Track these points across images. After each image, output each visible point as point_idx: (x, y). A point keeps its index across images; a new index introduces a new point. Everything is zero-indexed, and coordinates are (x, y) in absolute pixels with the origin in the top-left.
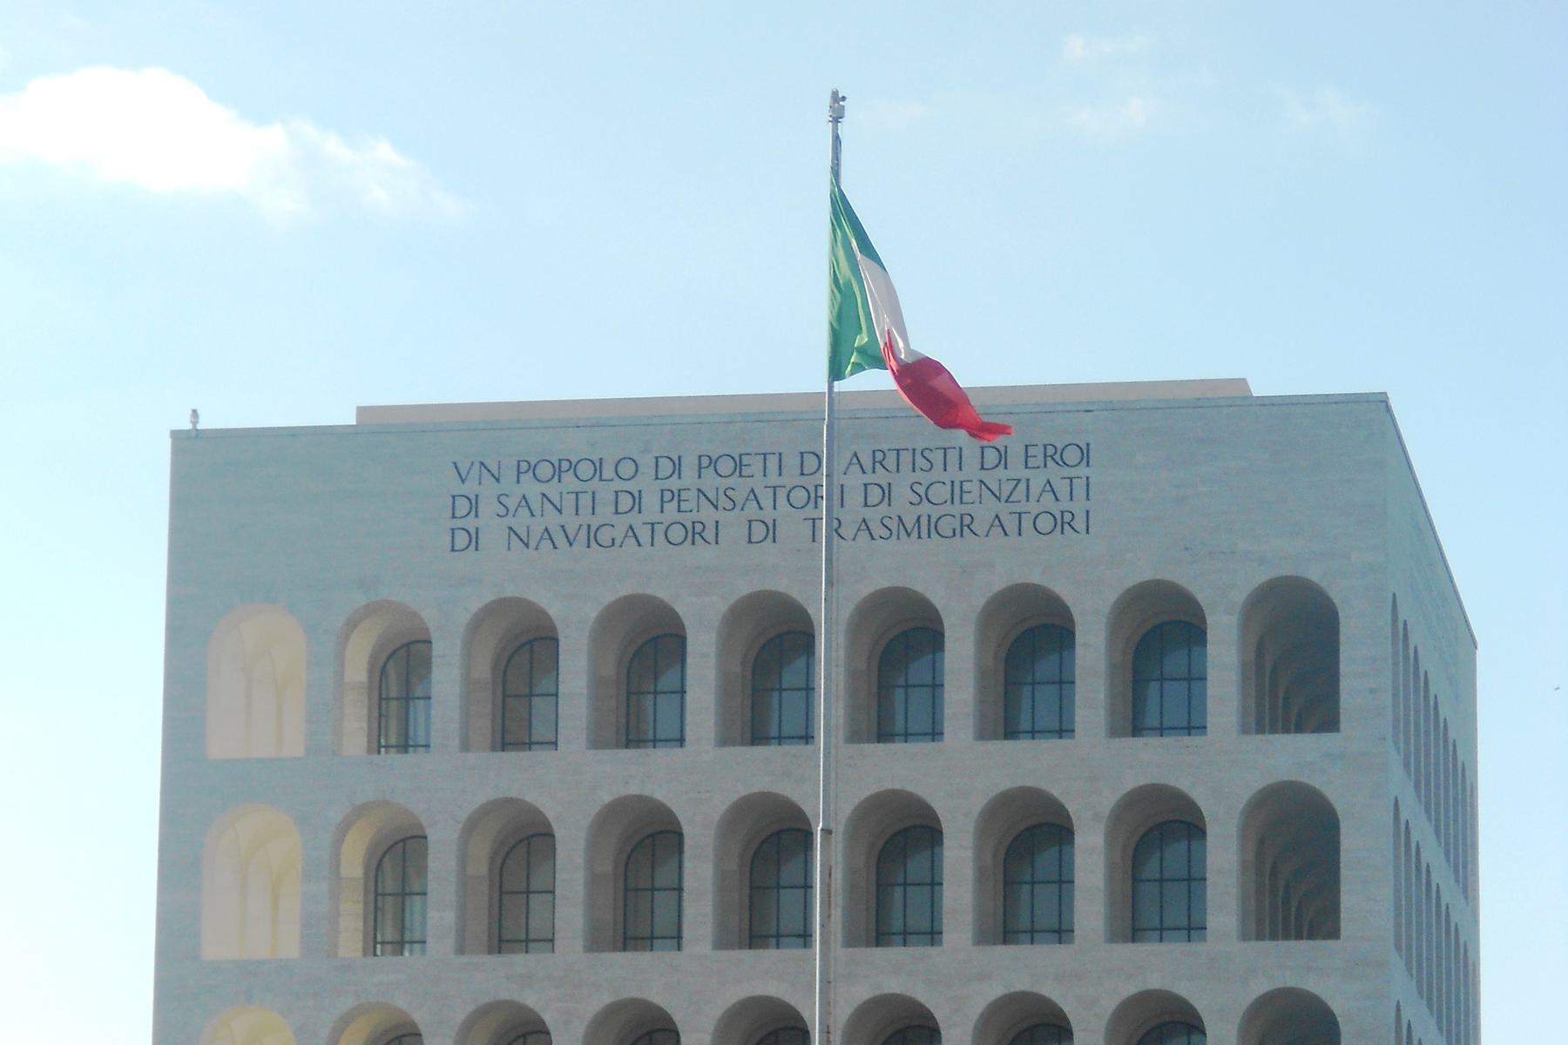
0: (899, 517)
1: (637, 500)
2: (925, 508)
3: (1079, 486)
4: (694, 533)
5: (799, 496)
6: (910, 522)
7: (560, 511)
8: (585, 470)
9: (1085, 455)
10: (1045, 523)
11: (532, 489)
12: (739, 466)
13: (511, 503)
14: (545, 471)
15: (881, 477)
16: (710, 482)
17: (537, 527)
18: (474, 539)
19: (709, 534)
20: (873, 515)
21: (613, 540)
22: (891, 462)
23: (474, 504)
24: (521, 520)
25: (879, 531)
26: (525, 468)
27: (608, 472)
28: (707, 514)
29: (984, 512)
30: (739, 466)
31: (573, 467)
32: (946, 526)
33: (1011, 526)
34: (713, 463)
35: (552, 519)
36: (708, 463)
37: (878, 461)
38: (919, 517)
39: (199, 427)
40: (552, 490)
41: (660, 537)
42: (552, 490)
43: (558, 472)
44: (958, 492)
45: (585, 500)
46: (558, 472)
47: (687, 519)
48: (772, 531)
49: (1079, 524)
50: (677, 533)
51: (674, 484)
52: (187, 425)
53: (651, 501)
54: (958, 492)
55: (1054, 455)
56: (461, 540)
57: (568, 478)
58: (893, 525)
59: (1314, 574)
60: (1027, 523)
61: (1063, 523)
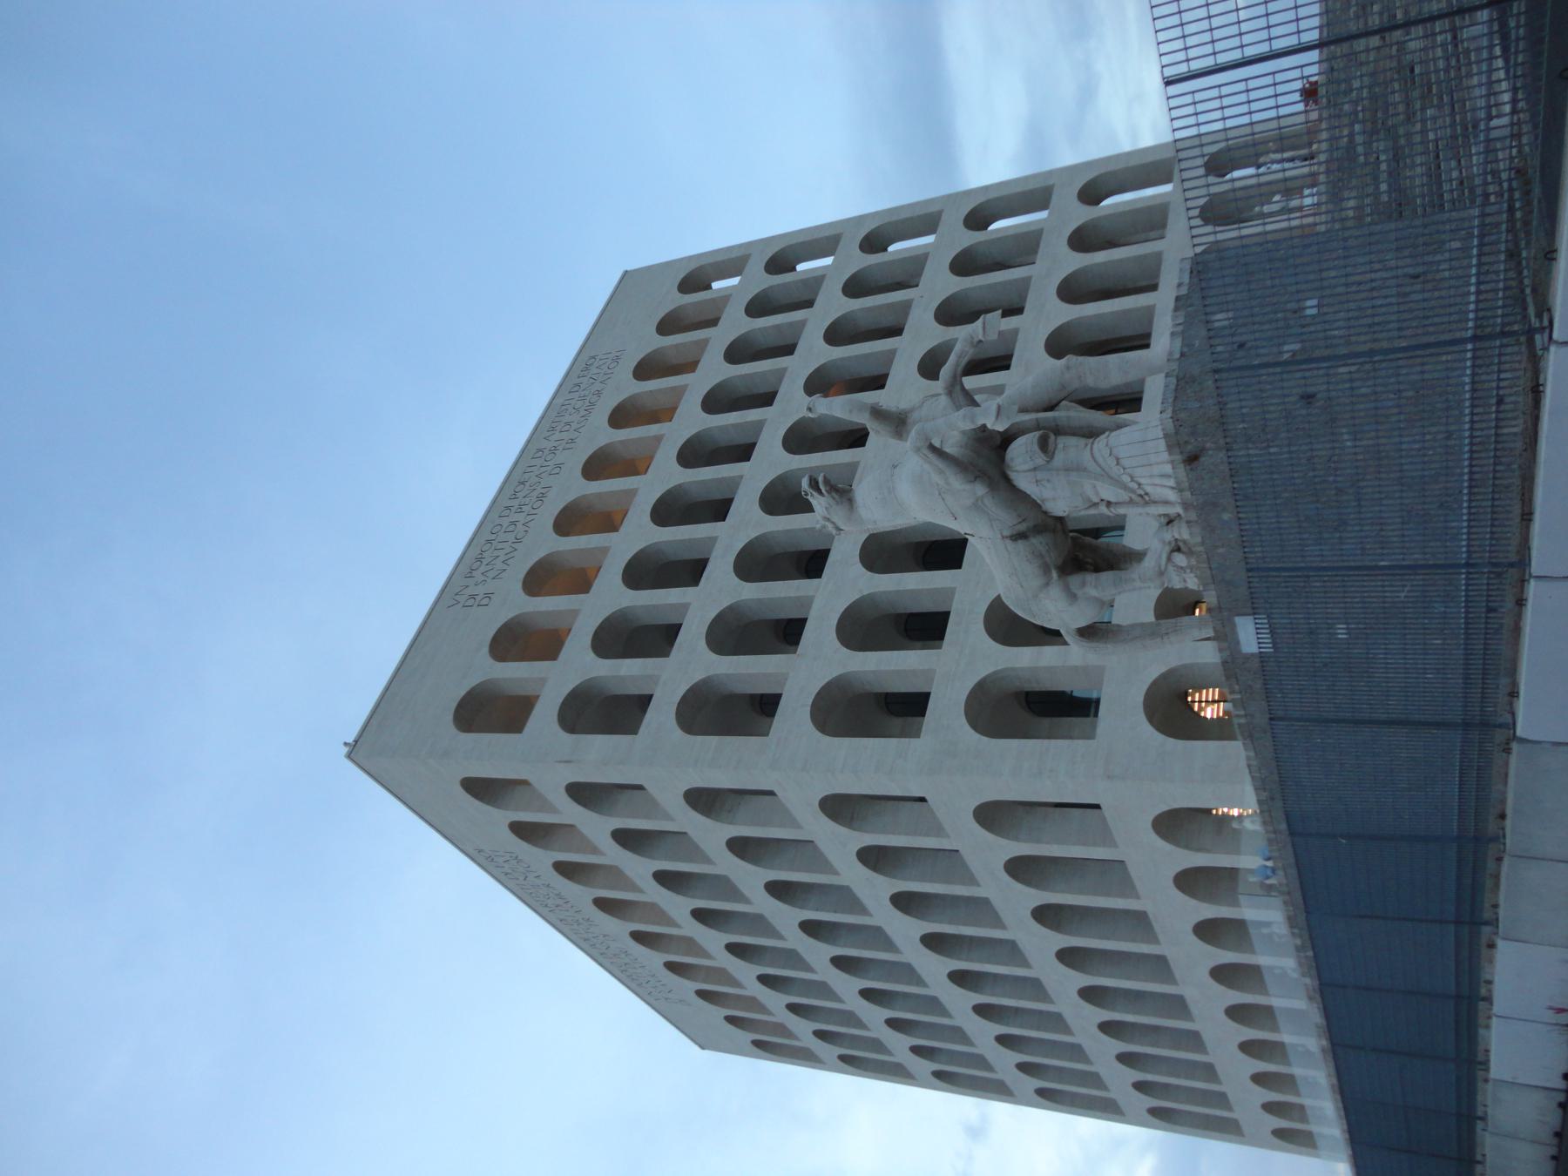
1: (513, 523)
4: (541, 498)
9: (593, 357)
11: (483, 569)
12: (522, 483)
17: (499, 565)
18: (488, 596)
19: (543, 491)
20: (574, 426)
23: (473, 597)
24: (491, 574)
25: (583, 424)
27: (493, 537)
28: (535, 494)
29: (597, 386)
35: (502, 558)
36: (514, 496)
41: (534, 511)
42: (485, 562)
44: (583, 398)
45: (500, 546)
47: (534, 499)
48: (559, 466)
56: (485, 601)
61: (617, 359)
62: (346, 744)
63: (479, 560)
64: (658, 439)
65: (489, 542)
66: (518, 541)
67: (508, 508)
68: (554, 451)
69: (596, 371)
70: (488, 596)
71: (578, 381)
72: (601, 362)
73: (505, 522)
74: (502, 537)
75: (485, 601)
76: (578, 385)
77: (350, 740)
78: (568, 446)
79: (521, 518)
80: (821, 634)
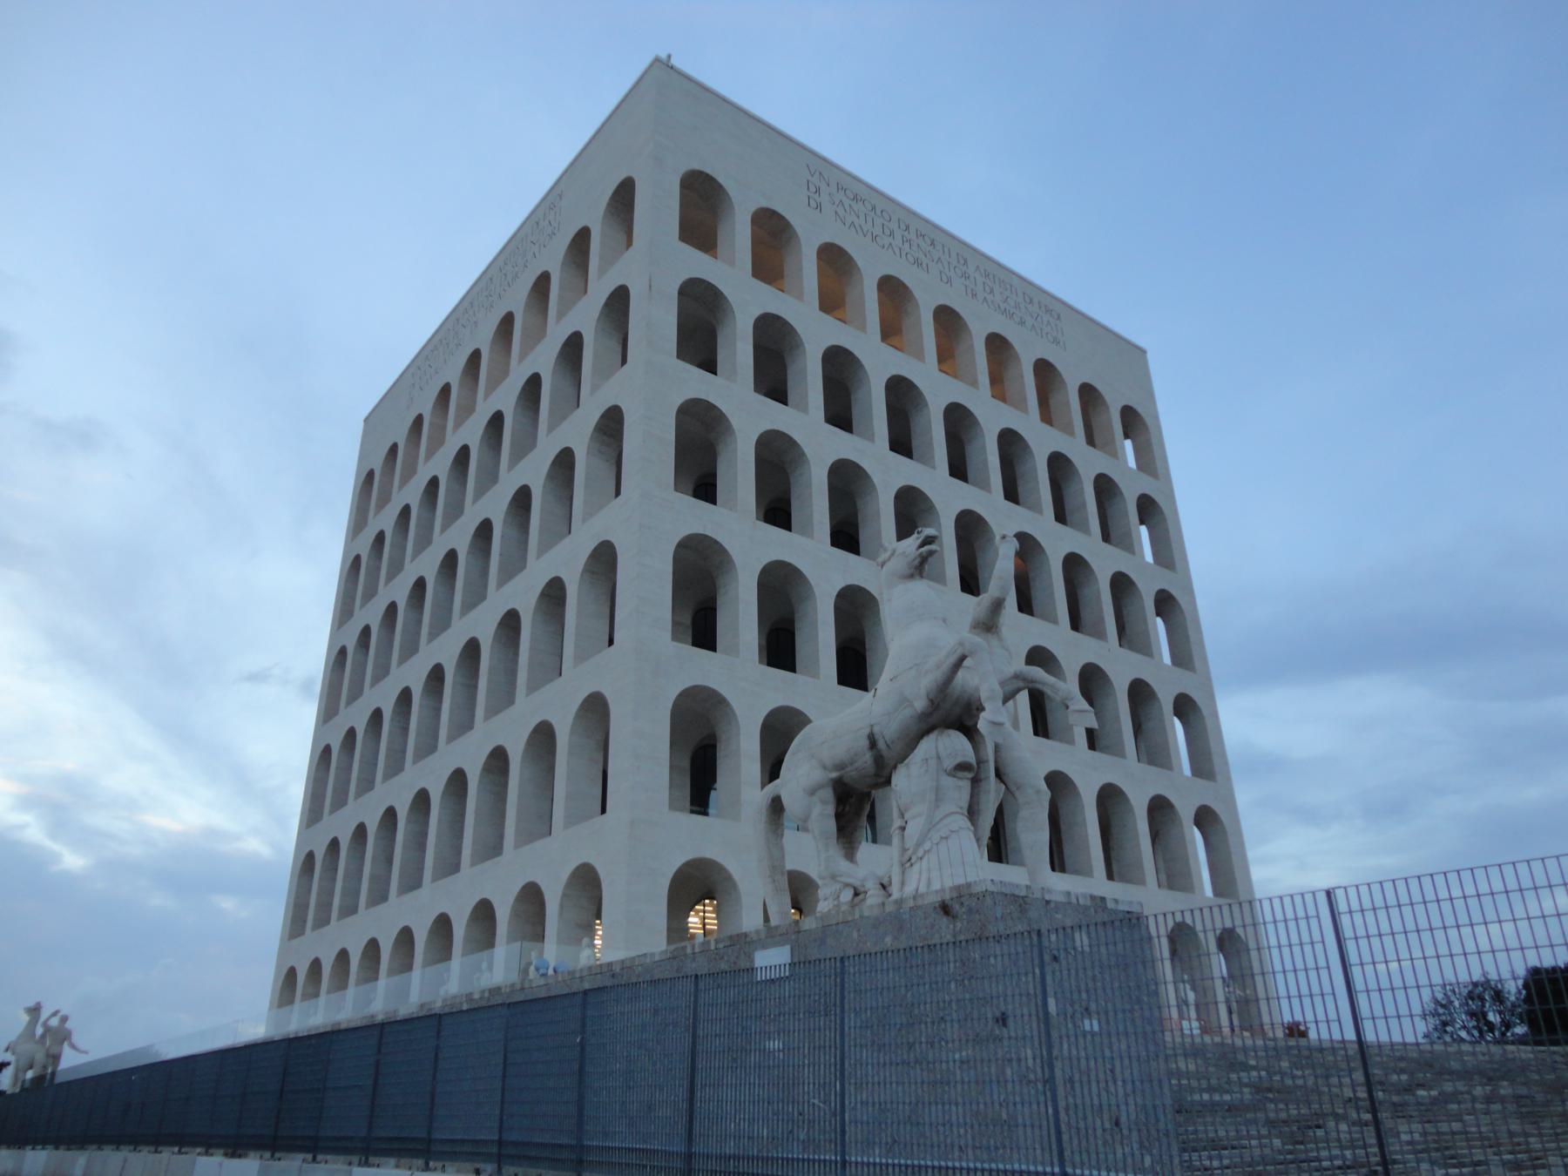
1: (892, 234)
4: (918, 263)
9: (1059, 318)
11: (847, 202)
12: (932, 243)
16: (920, 240)
18: (819, 207)
19: (924, 265)
20: (990, 297)
21: (883, 247)
23: (818, 191)
27: (878, 212)
28: (921, 256)
35: (856, 222)
42: (853, 204)
44: (1017, 306)
48: (949, 281)
54: (1017, 306)
55: (1048, 311)
56: (813, 204)
61: (1056, 341)
62: (669, 56)
63: (856, 198)
64: (974, 383)
65: (874, 208)
66: (874, 238)
67: (907, 228)
68: (965, 276)
70: (819, 207)
71: (1036, 301)
73: (893, 225)
74: (878, 221)
75: (813, 204)
76: (1031, 301)
77: (675, 62)
78: (969, 292)
79: (898, 242)
80: (775, 545)
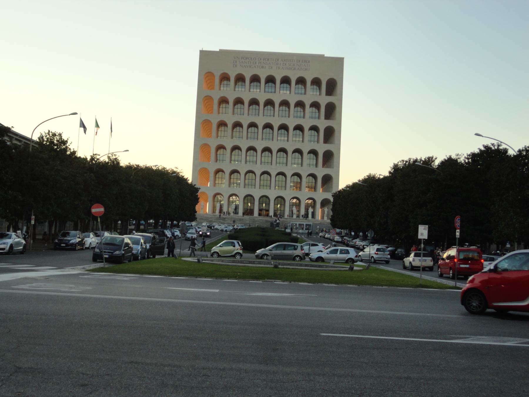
0: (287, 68)
1: (256, 63)
2: (290, 67)
3: (308, 66)
4: (263, 67)
5: (275, 64)
6: (288, 68)
7: (246, 63)
8: (250, 59)
9: (309, 62)
10: (304, 69)
12: (268, 60)
13: (241, 62)
14: (245, 58)
15: (285, 62)
16: (264, 61)
18: (236, 66)
22: (286, 61)
23: (236, 62)
26: (242, 58)
27: (252, 59)
30: (268, 60)
31: (248, 58)
32: (292, 69)
33: (300, 69)
34: (265, 59)
36: (264, 59)
37: (285, 60)
38: (289, 68)
39: (203, 50)
40: (246, 61)
42: (246, 61)
43: (246, 59)
44: (294, 65)
45: (249, 63)
46: (246, 59)
48: (272, 68)
49: (308, 70)
50: (260, 67)
51: (260, 61)
52: (201, 50)
53: (257, 63)
54: (294, 65)
55: (305, 61)
56: (234, 66)
57: (247, 59)
58: (286, 68)
59: (335, 78)
60: (302, 69)
61: (306, 69)
69: (303, 65)
72: (306, 65)
77: (204, 49)
